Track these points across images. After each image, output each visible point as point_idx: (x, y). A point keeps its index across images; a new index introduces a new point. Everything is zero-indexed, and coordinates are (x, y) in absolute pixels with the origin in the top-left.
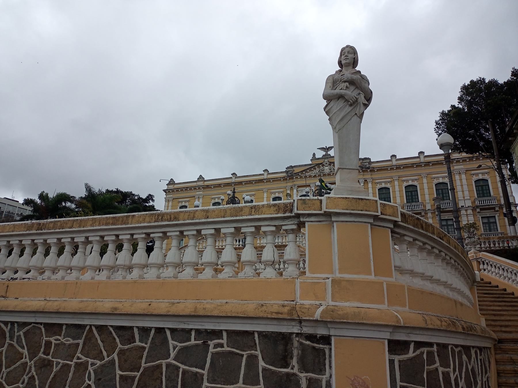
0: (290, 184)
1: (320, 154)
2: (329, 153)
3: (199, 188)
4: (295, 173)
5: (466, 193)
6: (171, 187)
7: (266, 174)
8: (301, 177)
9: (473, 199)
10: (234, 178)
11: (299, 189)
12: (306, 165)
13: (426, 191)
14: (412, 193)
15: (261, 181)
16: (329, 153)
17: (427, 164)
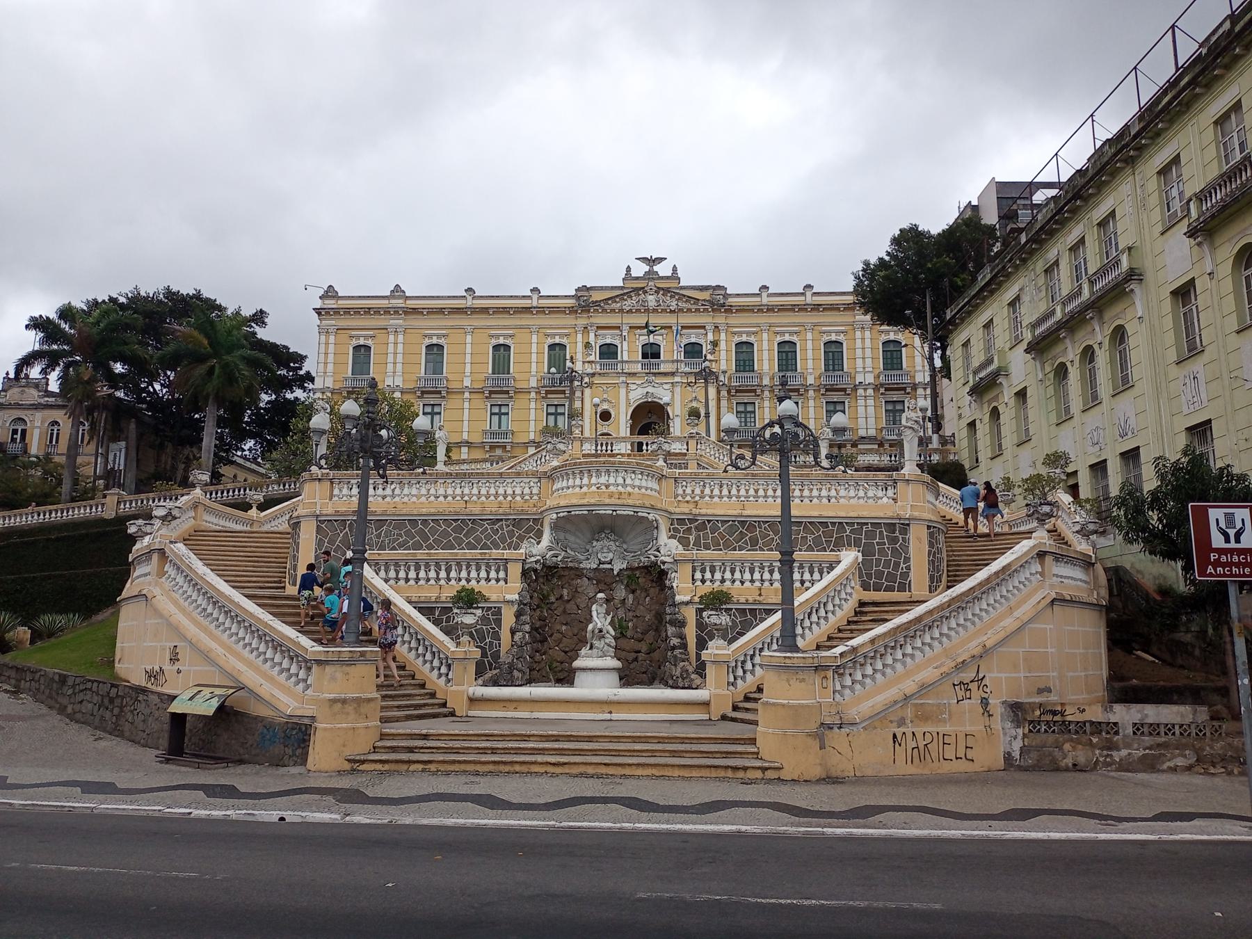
0: (582, 321)
1: (640, 270)
2: (656, 268)
3: (396, 312)
4: (593, 302)
5: (869, 362)
6: (330, 303)
7: (535, 297)
8: (604, 311)
9: (877, 372)
10: (470, 298)
11: (600, 332)
12: (613, 288)
13: (810, 353)
14: (787, 354)
15: (527, 310)
16: (656, 268)
17: (816, 308)
